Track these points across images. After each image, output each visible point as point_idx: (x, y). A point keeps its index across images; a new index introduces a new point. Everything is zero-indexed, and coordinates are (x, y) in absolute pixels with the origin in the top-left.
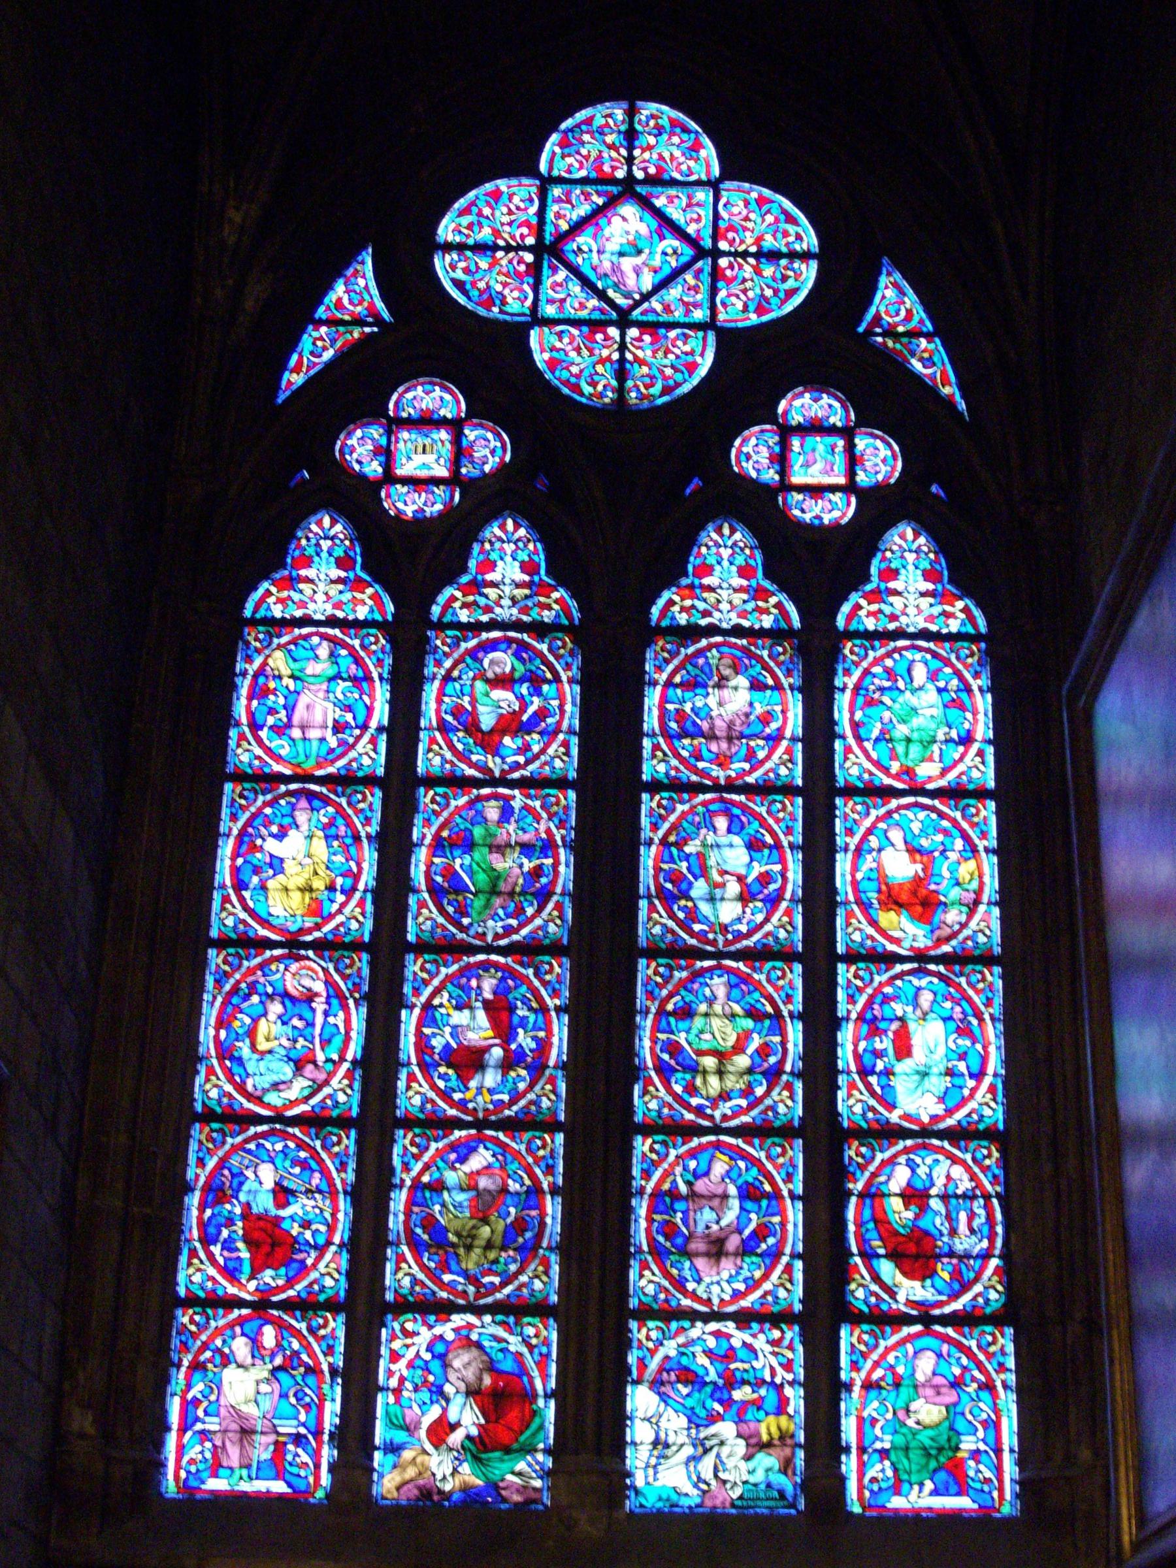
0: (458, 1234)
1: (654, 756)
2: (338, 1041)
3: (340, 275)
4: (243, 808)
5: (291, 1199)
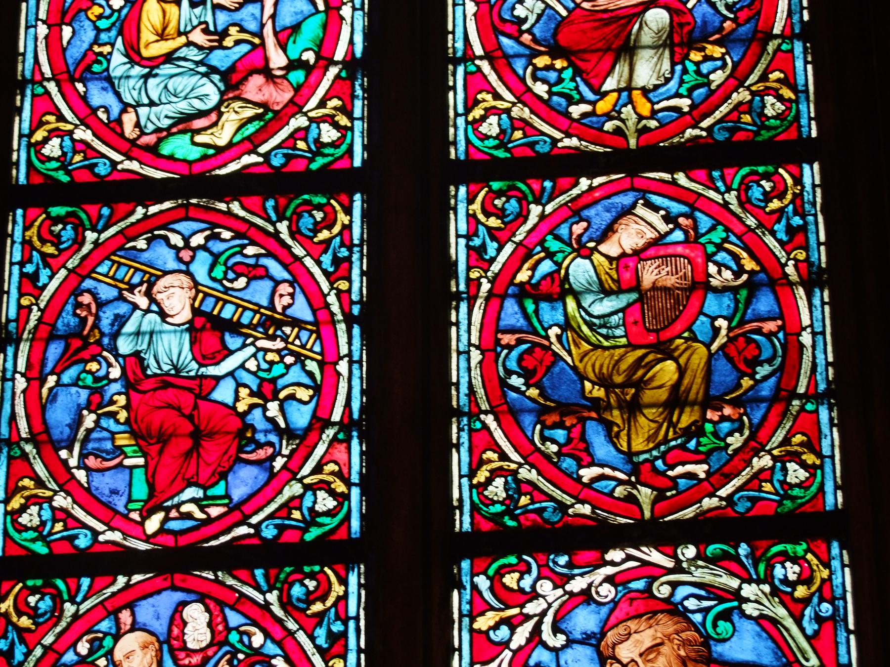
2: (312, 29)
5: (233, 342)
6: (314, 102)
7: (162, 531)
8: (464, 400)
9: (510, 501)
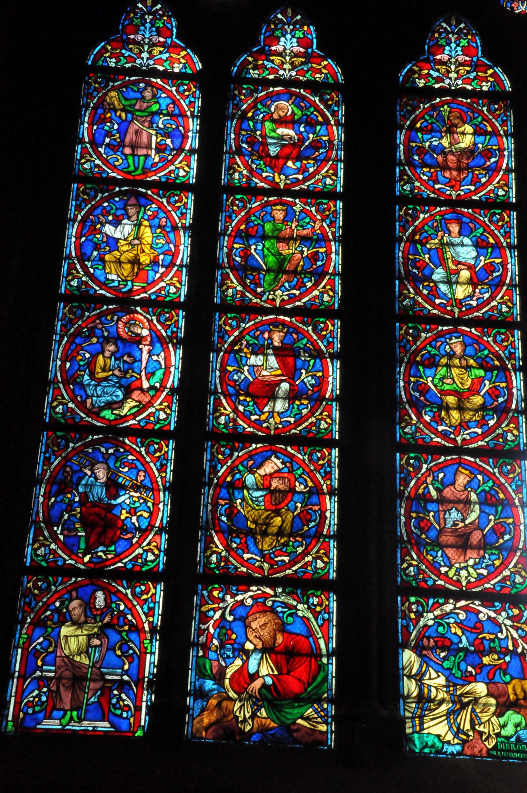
0: (254, 522)
1: (401, 179)
2: (159, 374)
4: (86, 202)
6: (158, 402)
7: (90, 561)
8: (204, 524)
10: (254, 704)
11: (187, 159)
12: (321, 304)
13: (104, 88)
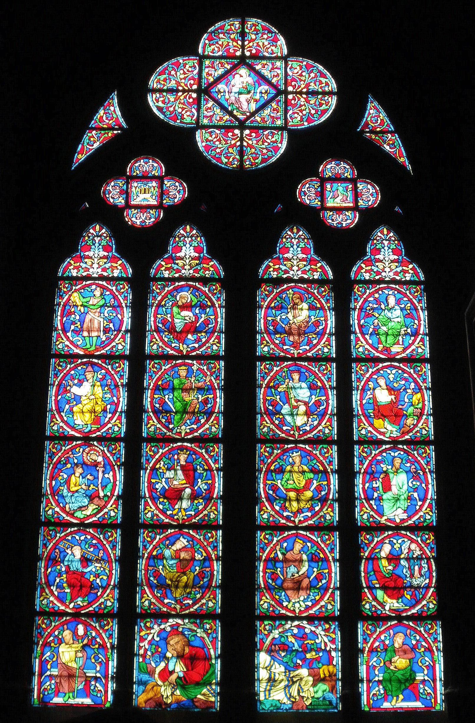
0: (171, 580)
2: (110, 486)
3: (102, 105)
5: (90, 564)
9: (149, 606)
10: (173, 688)
11: (123, 337)
12: (211, 434)
13: (69, 291)
